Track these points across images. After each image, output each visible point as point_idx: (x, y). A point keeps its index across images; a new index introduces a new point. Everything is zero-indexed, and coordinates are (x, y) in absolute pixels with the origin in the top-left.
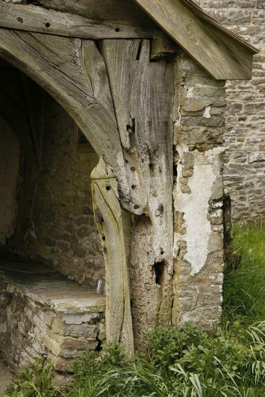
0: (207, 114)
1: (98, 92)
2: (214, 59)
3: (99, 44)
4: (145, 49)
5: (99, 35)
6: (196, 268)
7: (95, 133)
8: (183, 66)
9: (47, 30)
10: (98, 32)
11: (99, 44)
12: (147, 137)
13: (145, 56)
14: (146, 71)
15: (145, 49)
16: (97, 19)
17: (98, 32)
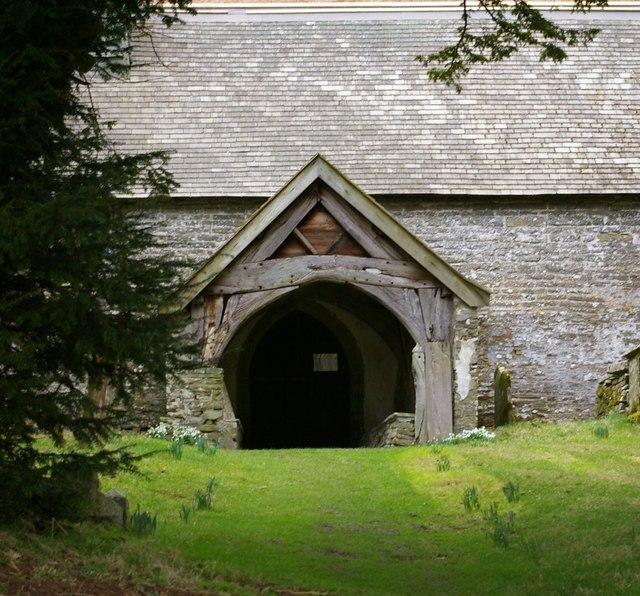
0: (468, 322)
1: (416, 313)
2: (471, 298)
3: (416, 290)
4: (438, 292)
5: (416, 287)
6: (463, 397)
7: (415, 330)
8: (455, 300)
9: (392, 285)
10: (416, 285)
11: (416, 290)
12: (439, 333)
13: (438, 296)
14: (438, 303)
15: (438, 292)
16: (417, 280)
17: (416, 285)
